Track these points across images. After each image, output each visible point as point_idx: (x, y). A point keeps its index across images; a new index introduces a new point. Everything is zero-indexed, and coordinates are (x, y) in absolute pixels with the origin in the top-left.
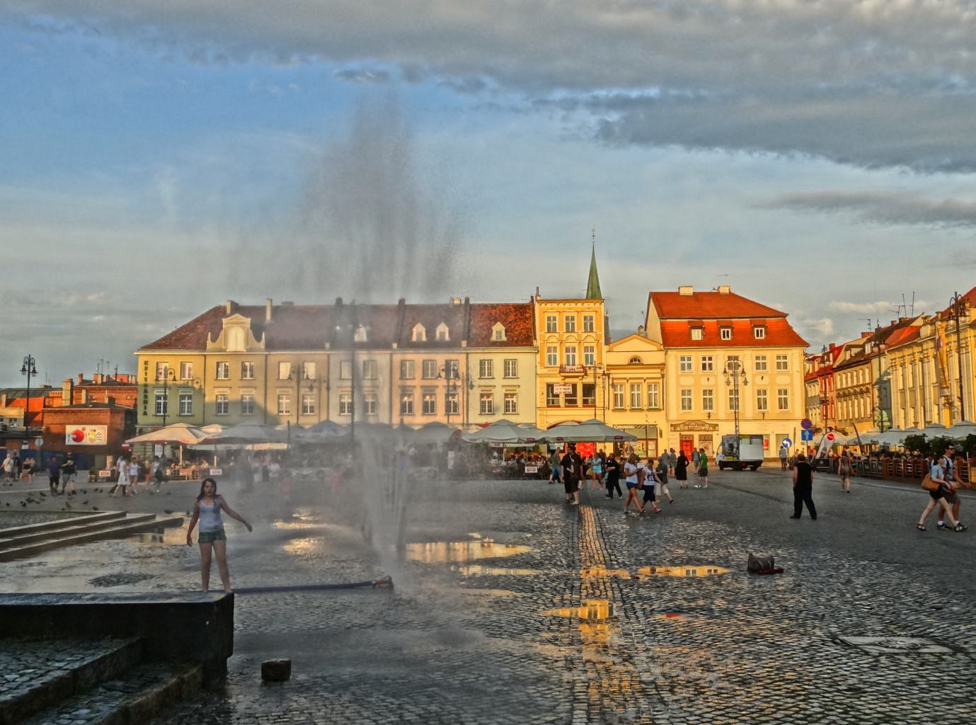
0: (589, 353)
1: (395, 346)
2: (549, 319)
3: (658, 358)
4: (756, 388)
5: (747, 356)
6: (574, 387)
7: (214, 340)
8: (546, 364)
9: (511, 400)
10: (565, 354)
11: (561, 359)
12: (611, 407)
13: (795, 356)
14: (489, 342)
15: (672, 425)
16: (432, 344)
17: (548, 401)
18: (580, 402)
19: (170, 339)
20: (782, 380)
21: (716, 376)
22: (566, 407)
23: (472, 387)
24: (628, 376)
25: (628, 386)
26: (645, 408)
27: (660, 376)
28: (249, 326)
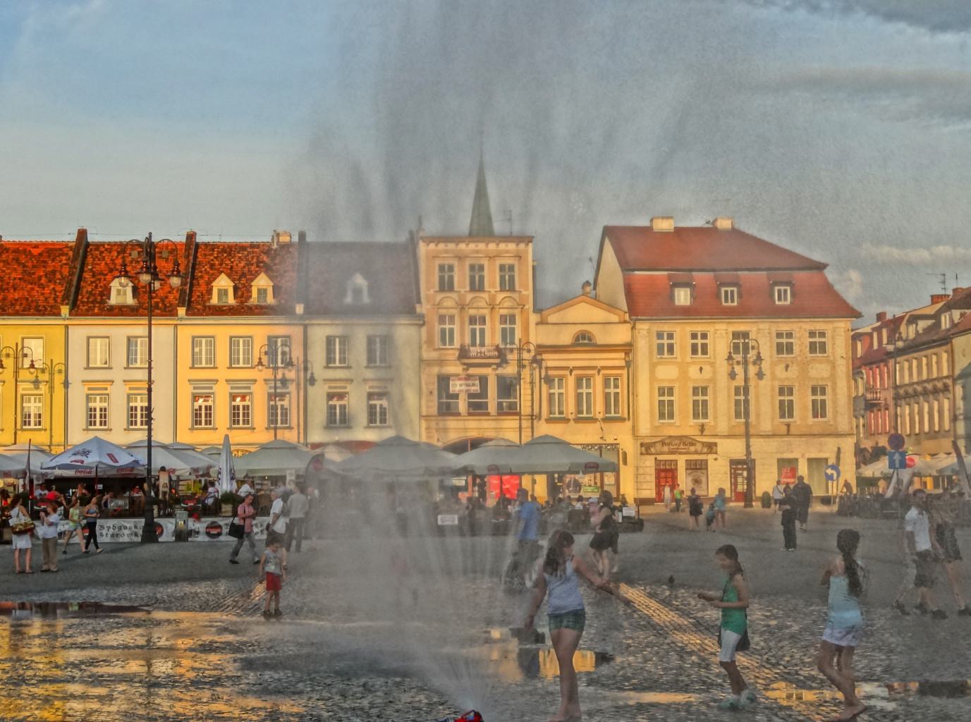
0: (508, 326)
1: (182, 311)
2: (442, 268)
3: (620, 335)
4: (777, 384)
5: (762, 332)
6: (483, 380)
8: (438, 343)
9: (378, 403)
10: (468, 328)
11: (461, 334)
13: (838, 332)
15: (642, 445)
16: (243, 308)
17: (440, 405)
18: (492, 408)
20: (819, 371)
21: (712, 364)
22: (470, 414)
23: (312, 381)
24: (572, 364)
25: (571, 381)
26: (600, 416)
27: (623, 363)
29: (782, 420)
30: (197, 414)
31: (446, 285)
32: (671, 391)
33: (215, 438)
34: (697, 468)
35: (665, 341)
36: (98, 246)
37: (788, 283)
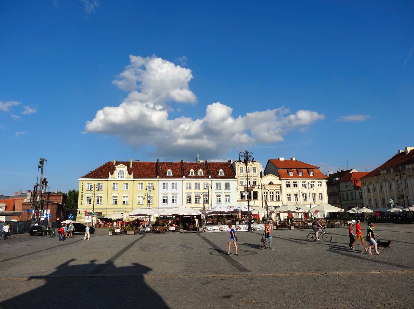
1: (184, 177)
6: (250, 193)
7: (112, 174)
9: (227, 198)
14: (218, 176)
16: (197, 177)
19: (92, 174)
26: (275, 200)
28: (126, 169)
30: (188, 200)
32: (290, 195)
35: (288, 184)
36: (161, 163)
37: (313, 171)
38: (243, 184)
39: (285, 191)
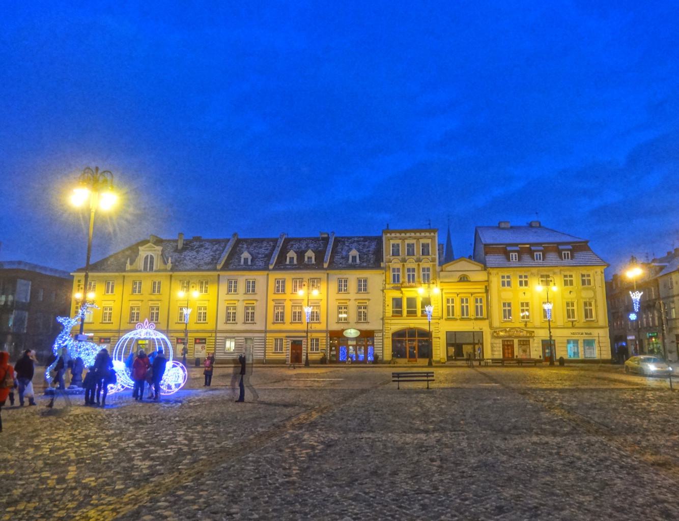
12: (445, 316)
16: (301, 265)
17: (393, 312)
27: (483, 291)
29: (569, 319)
30: (277, 316)
31: (396, 253)
32: (509, 305)
33: (303, 327)
34: (525, 343)
35: (506, 280)
38: (398, 281)
39: (499, 294)
